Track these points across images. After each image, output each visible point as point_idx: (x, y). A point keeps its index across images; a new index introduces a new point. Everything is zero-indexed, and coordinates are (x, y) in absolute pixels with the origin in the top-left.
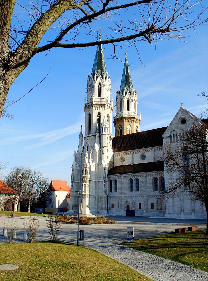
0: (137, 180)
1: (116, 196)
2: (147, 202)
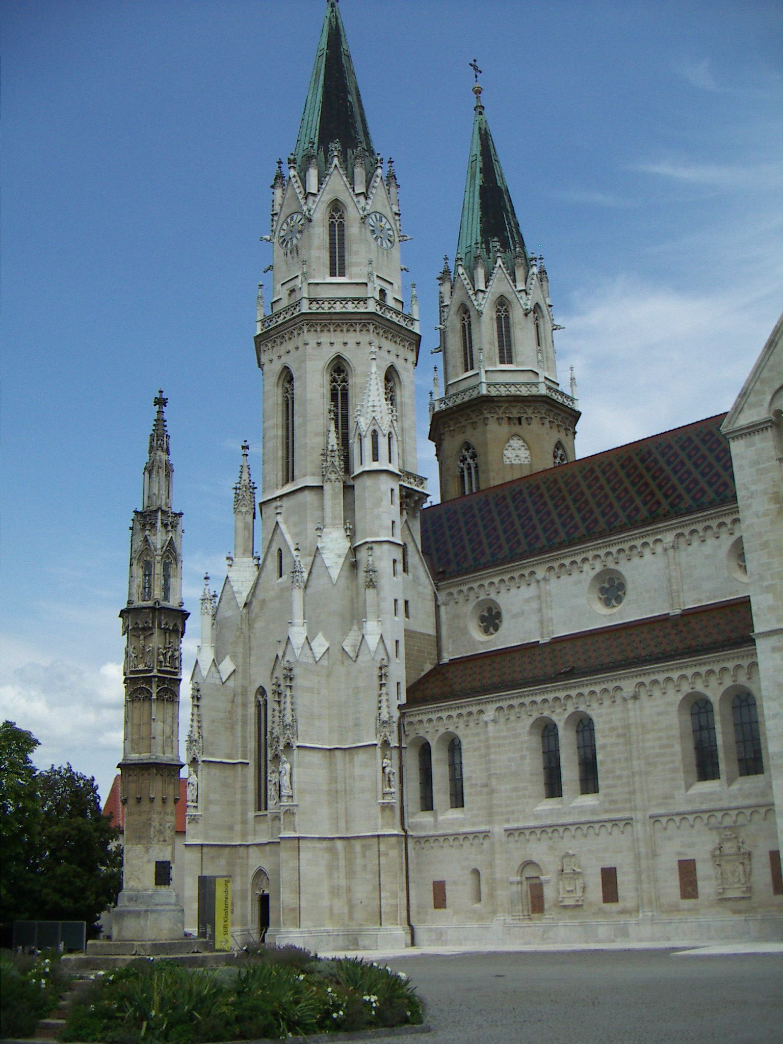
0: (584, 726)
1: (456, 836)
2: (654, 855)
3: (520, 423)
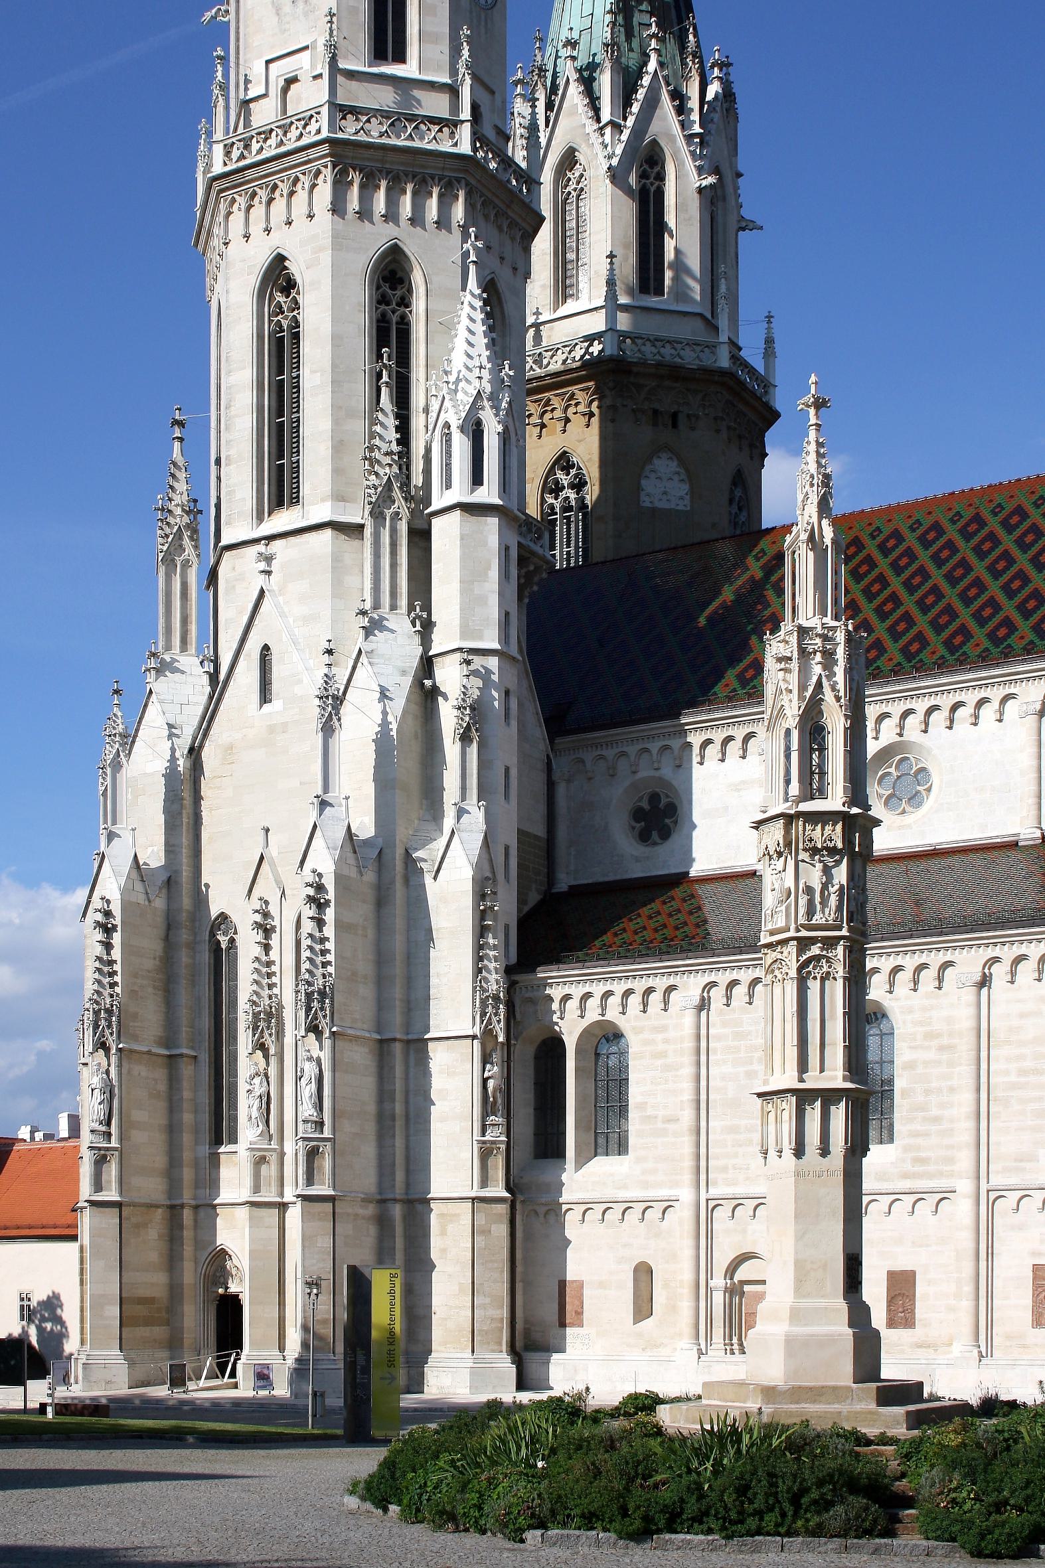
3: (675, 425)
